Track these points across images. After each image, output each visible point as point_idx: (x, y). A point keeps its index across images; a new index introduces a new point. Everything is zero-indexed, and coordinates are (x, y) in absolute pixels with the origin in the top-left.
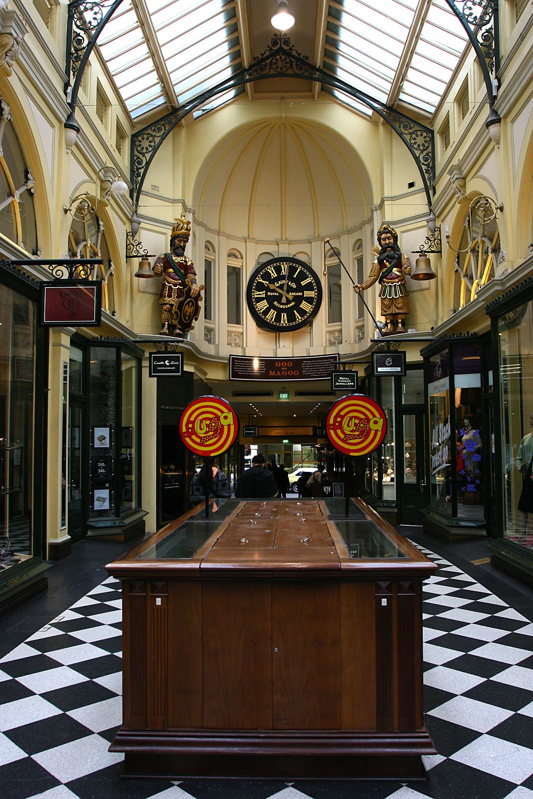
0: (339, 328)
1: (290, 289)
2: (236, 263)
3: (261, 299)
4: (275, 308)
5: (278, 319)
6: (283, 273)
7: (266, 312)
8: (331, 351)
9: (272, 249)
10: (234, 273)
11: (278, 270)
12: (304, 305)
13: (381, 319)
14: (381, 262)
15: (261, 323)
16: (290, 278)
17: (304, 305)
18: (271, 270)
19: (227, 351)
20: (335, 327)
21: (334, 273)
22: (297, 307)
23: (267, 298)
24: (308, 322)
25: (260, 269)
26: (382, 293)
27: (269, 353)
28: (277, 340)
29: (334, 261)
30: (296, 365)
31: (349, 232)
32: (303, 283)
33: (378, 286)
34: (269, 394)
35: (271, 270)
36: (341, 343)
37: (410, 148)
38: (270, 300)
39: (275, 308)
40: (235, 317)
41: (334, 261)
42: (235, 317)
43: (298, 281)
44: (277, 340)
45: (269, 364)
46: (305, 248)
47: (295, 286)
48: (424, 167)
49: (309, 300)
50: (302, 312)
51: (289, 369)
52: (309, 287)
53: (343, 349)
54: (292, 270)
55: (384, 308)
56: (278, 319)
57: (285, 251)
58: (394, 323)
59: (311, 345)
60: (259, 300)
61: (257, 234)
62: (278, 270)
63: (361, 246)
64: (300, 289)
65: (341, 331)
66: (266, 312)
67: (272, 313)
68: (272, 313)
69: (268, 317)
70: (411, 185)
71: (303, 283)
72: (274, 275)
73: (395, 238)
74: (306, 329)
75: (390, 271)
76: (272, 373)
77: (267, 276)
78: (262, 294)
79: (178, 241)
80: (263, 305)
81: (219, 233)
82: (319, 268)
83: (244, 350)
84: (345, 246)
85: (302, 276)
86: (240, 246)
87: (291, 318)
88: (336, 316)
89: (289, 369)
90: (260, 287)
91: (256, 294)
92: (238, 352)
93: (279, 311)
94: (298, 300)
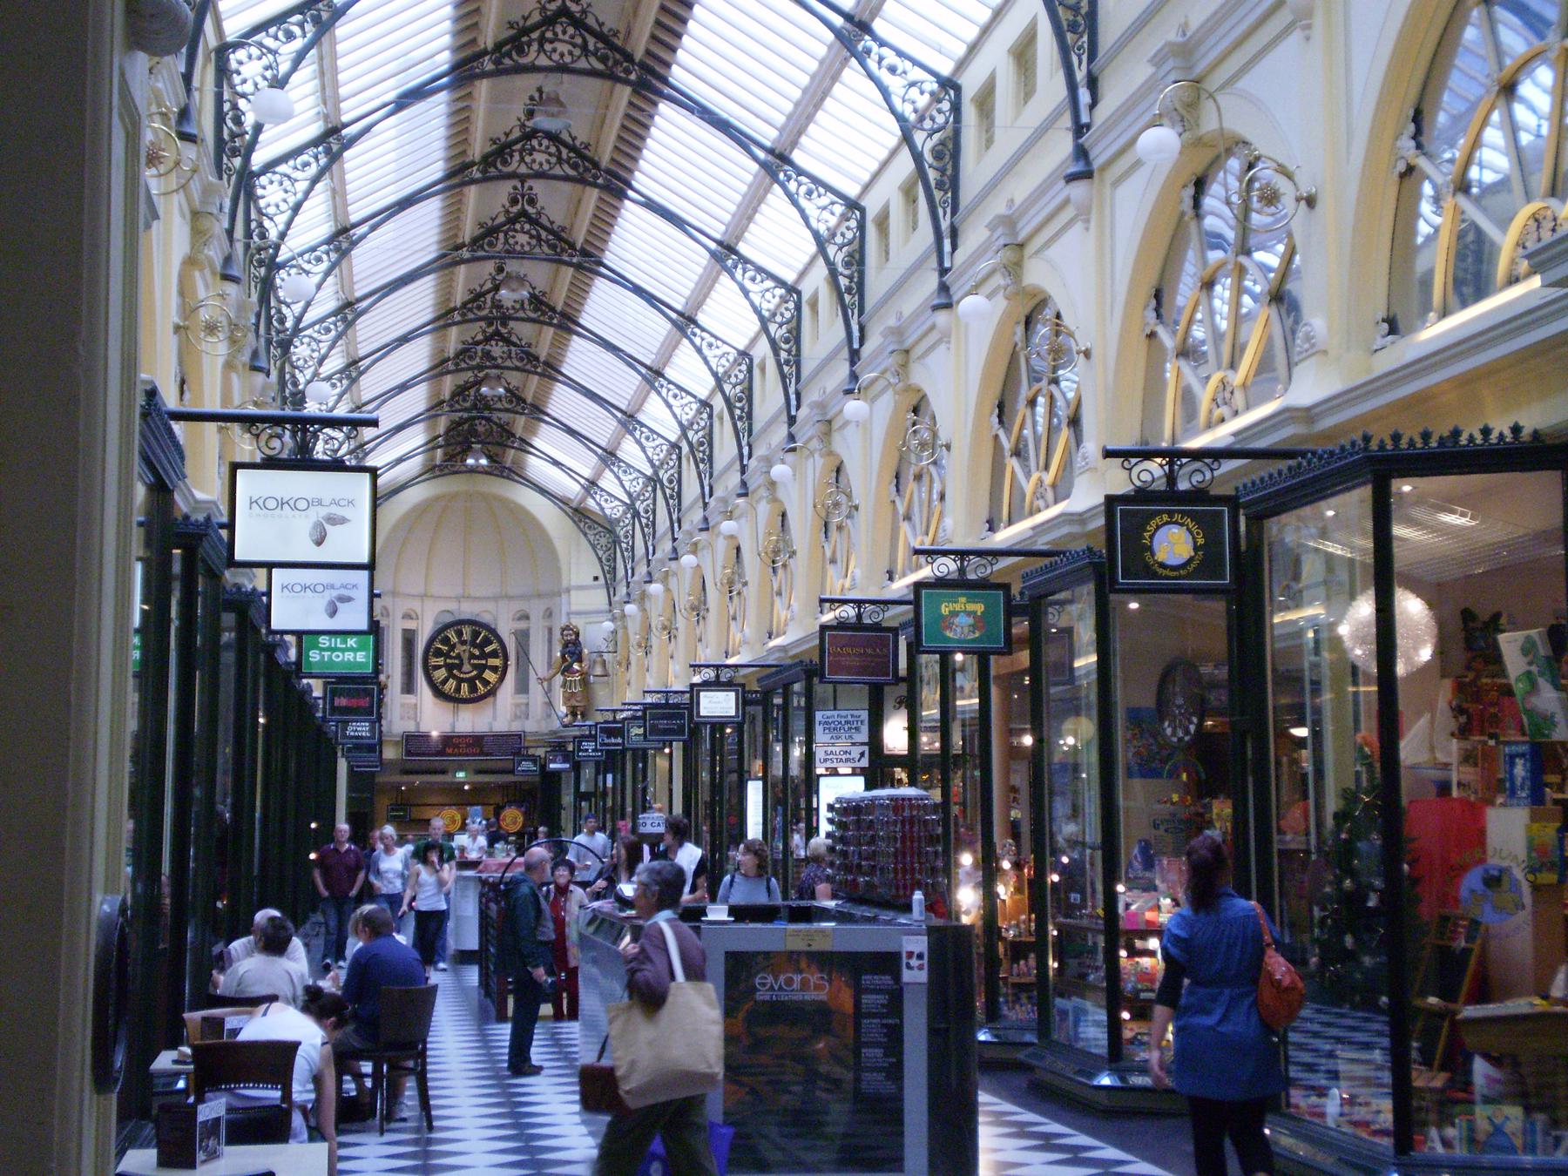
0: (525, 701)
1: (472, 656)
2: (411, 625)
3: (439, 667)
4: (455, 677)
5: (458, 690)
6: (465, 637)
7: (445, 681)
8: (516, 727)
9: (452, 606)
11: (460, 634)
12: (490, 676)
13: (563, 709)
14: (563, 656)
15: (438, 692)
16: (474, 645)
17: (490, 676)
20: (522, 699)
22: (479, 677)
23: (447, 666)
24: (492, 693)
25: (439, 634)
26: (564, 685)
27: (447, 729)
28: (455, 712)
29: (522, 625)
30: (477, 743)
31: (539, 596)
32: (488, 649)
33: (559, 679)
34: (443, 772)
36: (527, 718)
37: (594, 547)
38: (450, 668)
39: (455, 677)
40: (409, 687)
42: (409, 687)
43: (481, 646)
44: (455, 712)
45: (449, 741)
46: (490, 606)
47: (477, 653)
48: (606, 568)
49: (494, 669)
50: (486, 683)
51: (468, 745)
52: (494, 654)
53: (530, 726)
54: (476, 634)
55: (567, 699)
56: (458, 690)
57: (468, 610)
58: (574, 714)
59: (495, 718)
60: (437, 667)
61: (435, 589)
62: (460, 634)
63: (550, 615)
64: (484, 656)
65: (527, 704)
66: (445, 681)
67: (452, 684)
68: (452, 684)
69: (447, 687)
70: (596, 578)
71: (488, 649)
72: (455, 640)
73: (577, 634)
74: (490, 699)
75: (571, 665)
76: (449, 751)
77: (446, 641)
78: (440, 660)
80: (441, 674)
82: (506, 629)
83: (418, 724)
85: (487, 642)
86: (415, 605)
87: (473, 689)
88: (522, 687)
89: (468, 745)
90: (438, 653)
91: (434, 661)
92: (410, 727)
93: (460, 681)
94: (482, 668)
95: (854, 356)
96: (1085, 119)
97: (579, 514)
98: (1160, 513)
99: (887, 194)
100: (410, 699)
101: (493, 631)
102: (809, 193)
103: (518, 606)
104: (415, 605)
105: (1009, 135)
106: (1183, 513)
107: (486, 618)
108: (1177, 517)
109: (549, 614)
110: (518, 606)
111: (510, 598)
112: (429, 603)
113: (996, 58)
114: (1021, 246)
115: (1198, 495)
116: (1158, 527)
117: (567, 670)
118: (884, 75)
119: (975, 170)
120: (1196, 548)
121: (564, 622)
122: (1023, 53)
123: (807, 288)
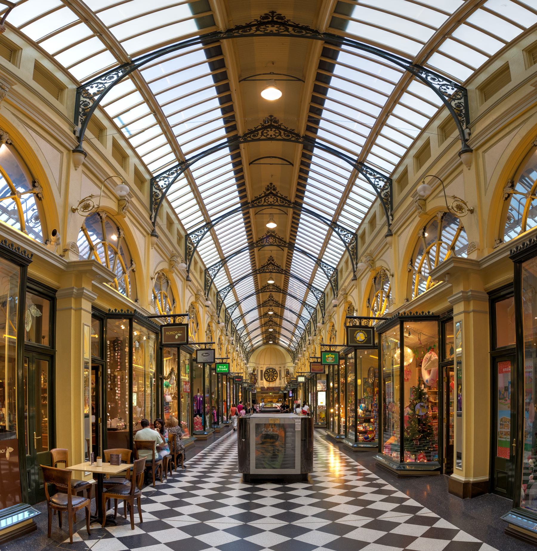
2: (262, 369)
8: (279, 386)
10: (262, 371)
12: (275, 377)
15: (266, 380)
17: (275, 377)
18: (268, 371)
19: (261, 386)
20: (280, 381)
21: (280, 371)
24: (275, 380)
25: (266, 370)
27: (268, 386)
29: (280, 369)
30: (273, 389)
31: (283, 364)
33: (286, 378)
35: (268, 371)
38: (268, 376)
40: (262, 379)
41: (280, 369)
42: (262, 379)
43: (273, 373)
45: (268, 388)
50: (274, 378)
52: (275, 374)
53: (282, 386)
54: (272, 370)
55: (287, 381)
57: (271, 366)
61: (265, 363)
64: (274, 374)
67: (269, 379)
68: (269, 379)
77: (268, 372)
79: (254, 371)
80: (267, 377)
81: (259, 364)
82: (277, 369)
84: (282, 366)
85: (274, 372)
86: (262, 366)
90: (266, 374)
91: (266, 375)
92: (262, 386)
94: (273, 376)
95: (323, 317)
96: (355, 270)
97: (288, 351)
98: (358, 330)
99: (328, 290)
100: (262, 381)
101: (275, 370)
102: (315, 291)
103: (279, 366)
104: (262, 366)
105: (345, 275)
106: (363, 330)
107: (274, 368)
108: (361, 331)
109: (284, 367)
110: (279, 366)
111: (277, 364)
112: (265, 366)
113: (343, 264)
114: (347, 294)
115: (366, 327)
116: (357, 333)
117: (287, 376)
118: (324, 268)
119: (340, 283)
120: (365, 338)
121: (286, 368)
122: (347, 262)
123: (317, 308)
